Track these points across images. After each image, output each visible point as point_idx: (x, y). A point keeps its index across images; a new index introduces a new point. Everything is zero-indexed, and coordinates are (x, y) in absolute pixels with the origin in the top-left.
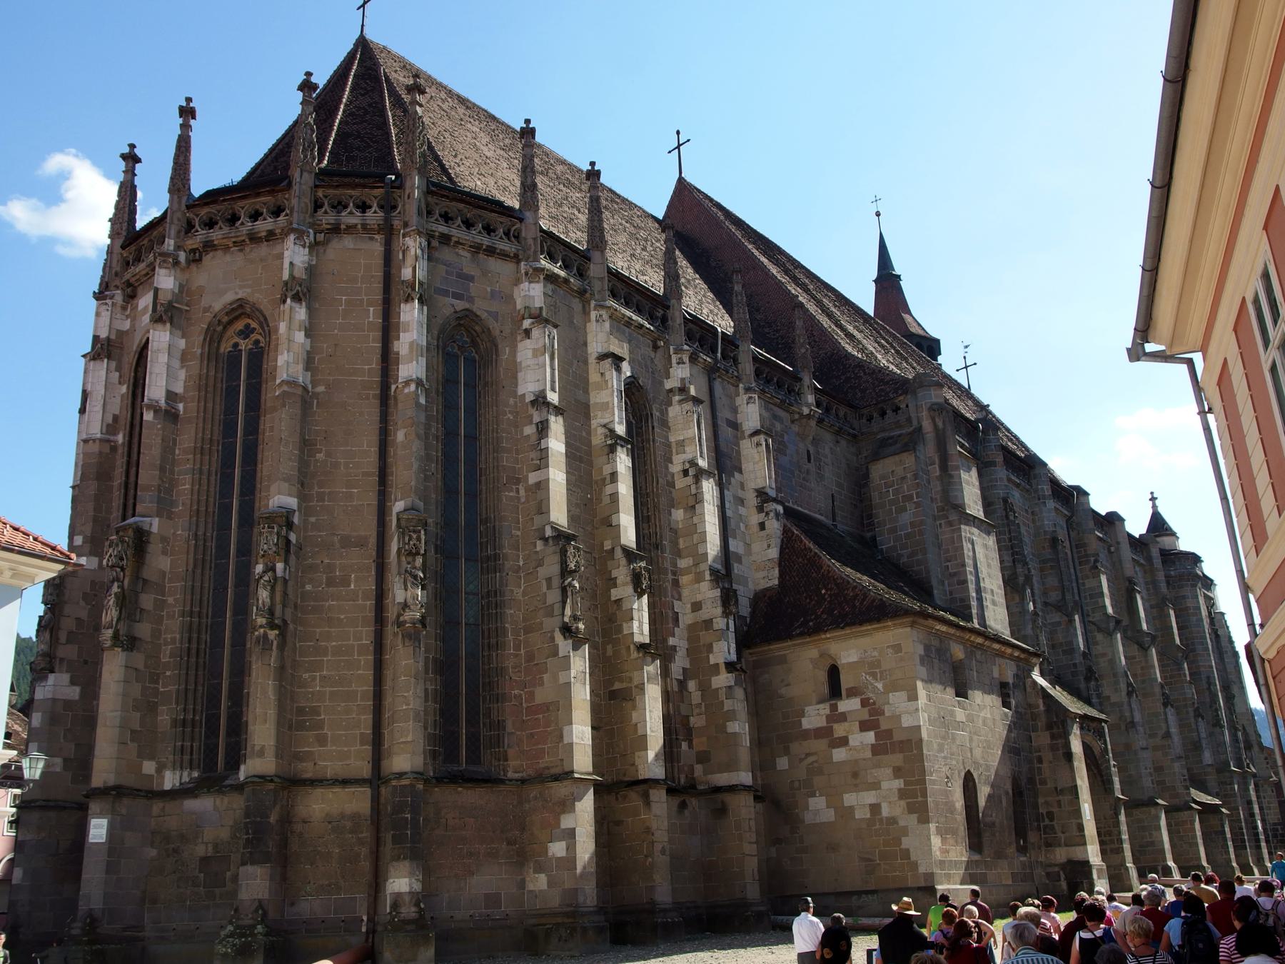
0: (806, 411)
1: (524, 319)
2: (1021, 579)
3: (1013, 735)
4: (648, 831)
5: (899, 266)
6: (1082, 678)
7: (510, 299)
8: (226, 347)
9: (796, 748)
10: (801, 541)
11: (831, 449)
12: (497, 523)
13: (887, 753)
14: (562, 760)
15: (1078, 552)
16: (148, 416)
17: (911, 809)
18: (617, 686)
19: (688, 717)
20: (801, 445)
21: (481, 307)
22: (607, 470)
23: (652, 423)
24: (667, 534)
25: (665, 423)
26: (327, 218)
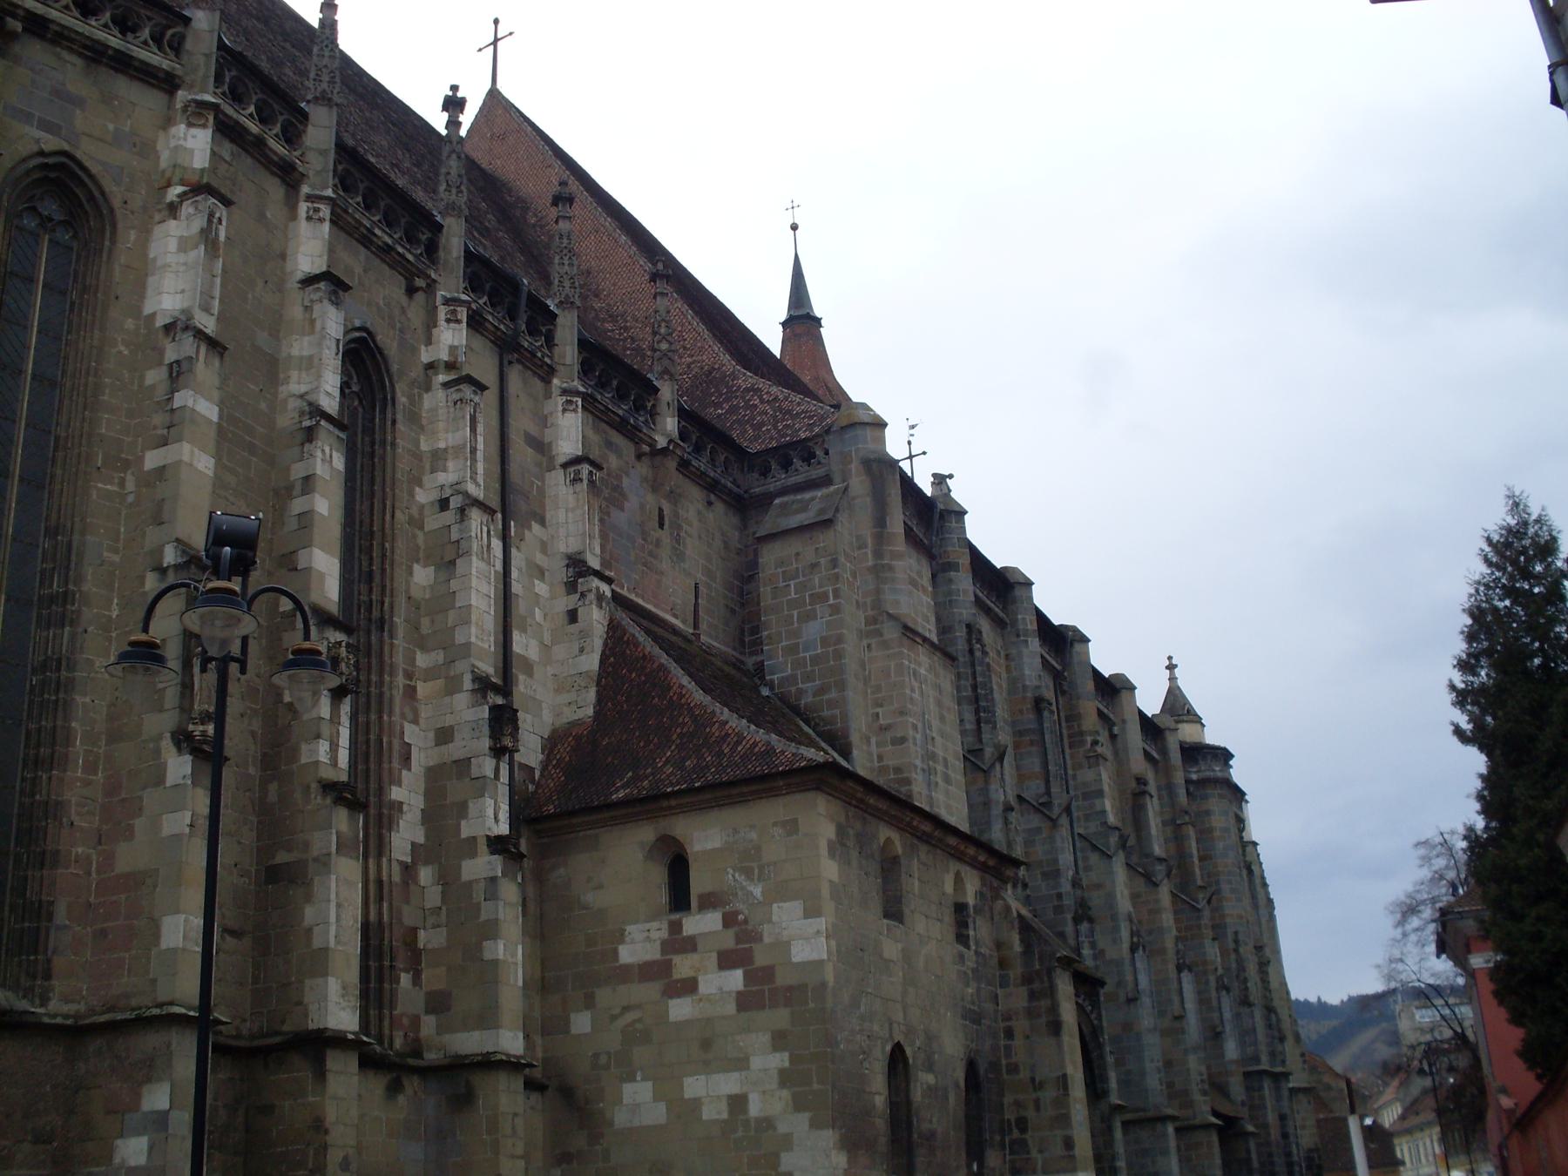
0: (662, 442)
1: (169, 185)
2: (989, 752)
3: (970, 990)
4: (319, 1126)
6: (1069, 917)
7: (146, 150)
9: (606, 997)
10: (637, 645)
11: (699, 513)
12: (76, 537)
13: (763, 1007)
14: (154, 981)
15: (1069, 728)
17: (799, 1105)
18: (282, 857)
19: (414, 931)
20: (651, 499)
21: (91, 154)
22: (298, 471)
23: (394, 414)
24: (401, 602)
25: (414, 418)
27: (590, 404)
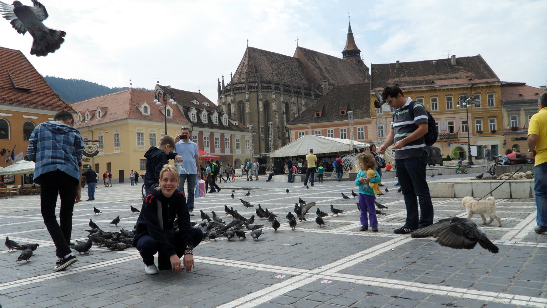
5: (353, 31)
8: (239, 105)
16: (232, 115)
21: (268, 99)
25: (291, 107)
26: (250, 90)
27: (305, 98)
